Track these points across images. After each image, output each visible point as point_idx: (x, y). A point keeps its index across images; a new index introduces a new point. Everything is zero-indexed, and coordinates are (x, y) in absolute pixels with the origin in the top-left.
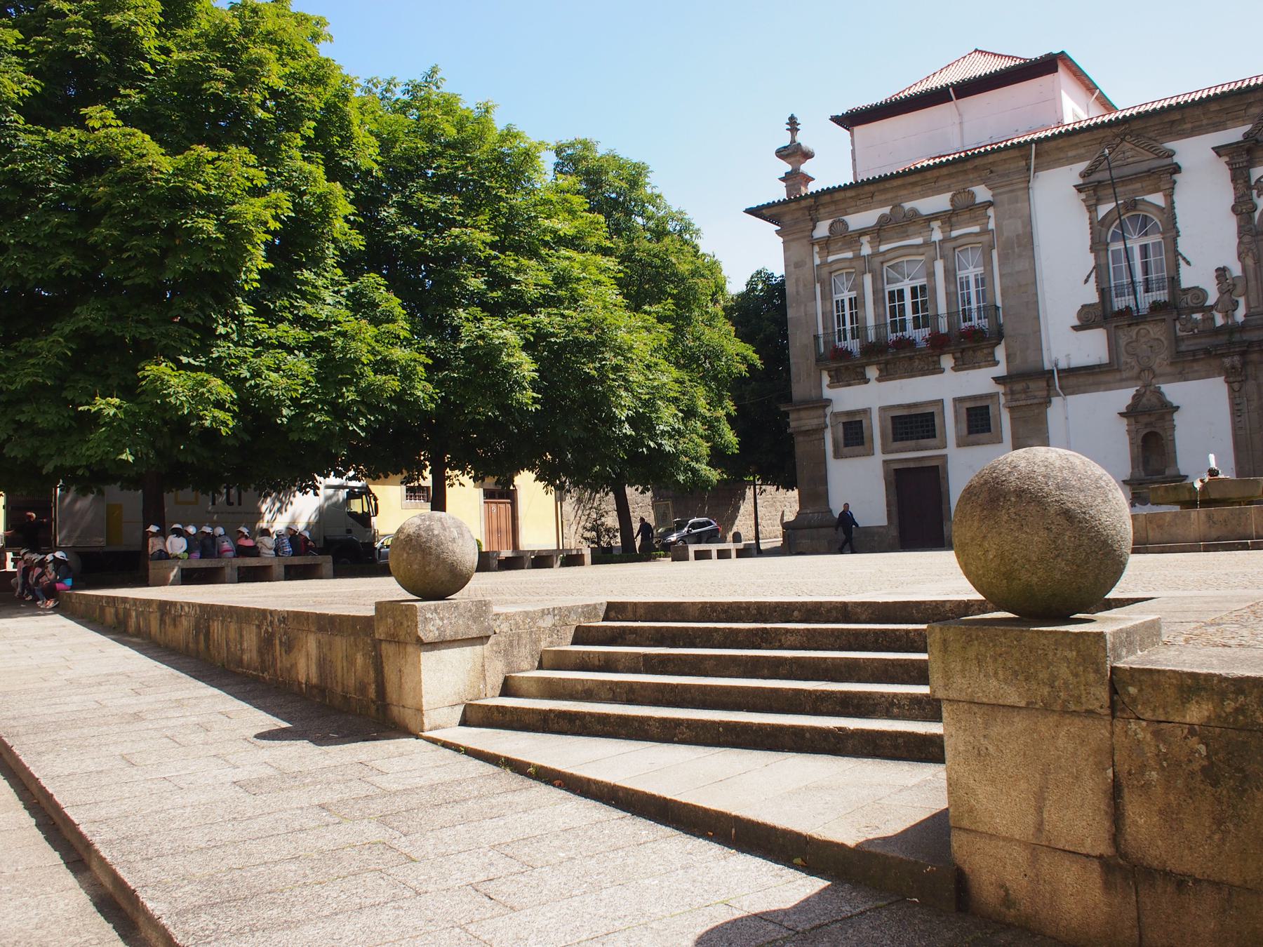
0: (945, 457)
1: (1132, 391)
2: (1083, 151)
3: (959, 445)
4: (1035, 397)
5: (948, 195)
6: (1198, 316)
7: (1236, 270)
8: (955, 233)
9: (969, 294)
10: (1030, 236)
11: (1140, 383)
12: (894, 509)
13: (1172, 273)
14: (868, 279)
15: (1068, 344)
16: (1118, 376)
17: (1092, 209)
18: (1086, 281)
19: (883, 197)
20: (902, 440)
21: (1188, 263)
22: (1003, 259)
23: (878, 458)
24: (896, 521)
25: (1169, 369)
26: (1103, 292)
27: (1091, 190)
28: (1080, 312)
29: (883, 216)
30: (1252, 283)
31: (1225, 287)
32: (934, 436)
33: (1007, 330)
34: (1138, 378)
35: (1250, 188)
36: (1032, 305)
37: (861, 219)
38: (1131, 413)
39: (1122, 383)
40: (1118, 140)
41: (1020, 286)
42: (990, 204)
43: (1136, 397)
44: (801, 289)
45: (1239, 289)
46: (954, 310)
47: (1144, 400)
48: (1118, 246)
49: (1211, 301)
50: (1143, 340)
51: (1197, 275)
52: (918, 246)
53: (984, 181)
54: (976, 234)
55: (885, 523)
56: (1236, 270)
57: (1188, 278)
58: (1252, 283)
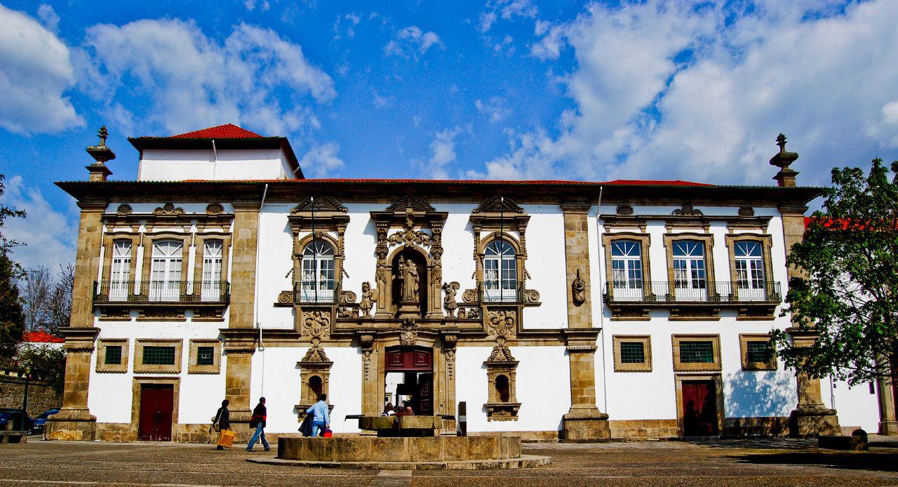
0: (177, 379)
1: (307, 349)
5: (206, 205)
6: (350, 309)
7: (374, 286)
12: (137, 412)
13: (337, 281)
14: (141, 250)
20: (149, 363)
21: (348, 277)
22: (237, 252)
23: (130, 375)
24: (137, 420)
26: (296, 285)
27: (296, 223)
28: (281, 294)
30: (382, 294)
31: (366, 294)
32: (173, 363)
33: (233, 299)
36: (252, 286)
37: (139, 209)
41: (245, 272)
43: (310, 353)
44: (90, 247)
46: (198, 280)
48: (310, 258)
51: (352, 284)
55: (129, 421)
56: (374, 286)
57: (346, 286)
58: (382, 294)
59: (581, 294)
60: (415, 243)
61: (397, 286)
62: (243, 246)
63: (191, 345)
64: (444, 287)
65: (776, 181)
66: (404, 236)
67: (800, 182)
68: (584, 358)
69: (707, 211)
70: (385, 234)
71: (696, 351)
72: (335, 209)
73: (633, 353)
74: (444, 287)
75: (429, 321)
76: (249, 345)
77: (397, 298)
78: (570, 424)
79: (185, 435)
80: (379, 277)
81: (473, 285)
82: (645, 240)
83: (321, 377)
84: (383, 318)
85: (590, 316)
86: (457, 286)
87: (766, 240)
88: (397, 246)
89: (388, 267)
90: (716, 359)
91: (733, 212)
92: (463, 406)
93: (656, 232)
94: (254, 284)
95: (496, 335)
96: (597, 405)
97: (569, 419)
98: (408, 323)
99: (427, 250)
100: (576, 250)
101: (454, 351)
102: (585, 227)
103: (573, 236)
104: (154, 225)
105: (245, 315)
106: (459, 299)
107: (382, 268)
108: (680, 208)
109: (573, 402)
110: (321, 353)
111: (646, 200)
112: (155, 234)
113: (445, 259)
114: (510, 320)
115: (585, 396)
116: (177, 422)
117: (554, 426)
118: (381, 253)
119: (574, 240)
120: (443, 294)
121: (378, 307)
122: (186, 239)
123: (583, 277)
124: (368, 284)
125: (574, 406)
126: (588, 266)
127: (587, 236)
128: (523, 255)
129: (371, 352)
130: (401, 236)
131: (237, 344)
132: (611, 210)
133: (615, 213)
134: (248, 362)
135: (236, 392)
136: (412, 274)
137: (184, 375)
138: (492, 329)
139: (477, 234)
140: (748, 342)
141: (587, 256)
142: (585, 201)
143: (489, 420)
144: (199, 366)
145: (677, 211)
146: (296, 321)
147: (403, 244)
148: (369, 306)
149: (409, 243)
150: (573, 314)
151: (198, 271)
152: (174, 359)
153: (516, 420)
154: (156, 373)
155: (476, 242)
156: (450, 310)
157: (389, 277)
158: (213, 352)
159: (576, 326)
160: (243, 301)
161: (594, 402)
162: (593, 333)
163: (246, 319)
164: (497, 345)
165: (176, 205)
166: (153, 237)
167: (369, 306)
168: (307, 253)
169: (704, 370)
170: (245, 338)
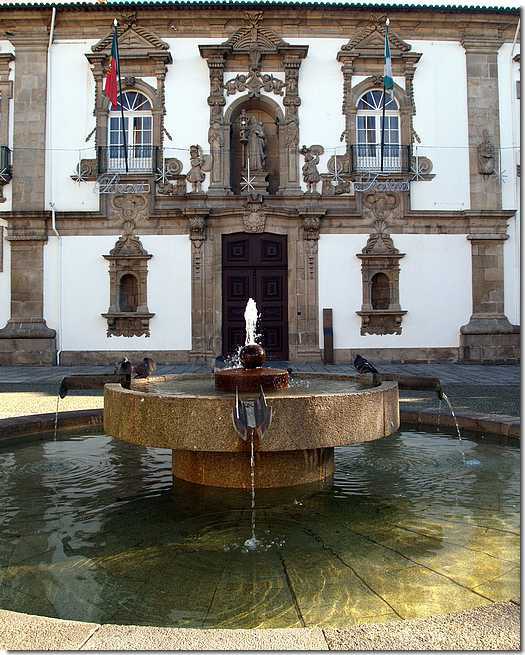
1: (116, 238)
4: (34, 234)
6: (174, 182)
7: (206, 148)
11: (123, 232)
15: (66, 192)
18: (87, 140)
22: (19, 107)
25: (148, 223)
26: (100, 150)
30: (217, 162)
34: (122, 228)
35: (222, 86)
39: (108, 231)
40: (126, 26)
41: (30, 134)
42: (11, 58)
43: (119, 244)
45: (207, 166)
48: (117, 114)
51: (176, 148)
56: (206, 148)
58: (217, 162)
60: (263, 92)
61: (236, 144)
64: (303, 152)
74: (305, 151)
75: (281, 198)
78: (472, 339)
80: (211, 140)
83: (136, 275)
84: (220, 194)
85: (499, 196)
92: (328, 313)
95: (374, 218)
96: (507, 313)
99: (278, 100)
100: (482, 104)
102: (494, 72)
103: (477, 84)
105: (32, 193)
106: (322, 168)
107: (216, 126)
110: (138, 243)
114: (392, 198)
118: (216, 102)
120: (302, 162)
121: (212, 180)
123: (493, 141)
126: (497, 126)
127: (497, 84)
139: (347, 77)
141: (497, 113)
143: (362, 334)
147: (246, 92)
150: (477, 191)
153: (399, 333)
155: (347, 87)
159: (480, 207)
161: (501, 309)
163: (34, 197)
164: (374, 231)
168: (115, 108)
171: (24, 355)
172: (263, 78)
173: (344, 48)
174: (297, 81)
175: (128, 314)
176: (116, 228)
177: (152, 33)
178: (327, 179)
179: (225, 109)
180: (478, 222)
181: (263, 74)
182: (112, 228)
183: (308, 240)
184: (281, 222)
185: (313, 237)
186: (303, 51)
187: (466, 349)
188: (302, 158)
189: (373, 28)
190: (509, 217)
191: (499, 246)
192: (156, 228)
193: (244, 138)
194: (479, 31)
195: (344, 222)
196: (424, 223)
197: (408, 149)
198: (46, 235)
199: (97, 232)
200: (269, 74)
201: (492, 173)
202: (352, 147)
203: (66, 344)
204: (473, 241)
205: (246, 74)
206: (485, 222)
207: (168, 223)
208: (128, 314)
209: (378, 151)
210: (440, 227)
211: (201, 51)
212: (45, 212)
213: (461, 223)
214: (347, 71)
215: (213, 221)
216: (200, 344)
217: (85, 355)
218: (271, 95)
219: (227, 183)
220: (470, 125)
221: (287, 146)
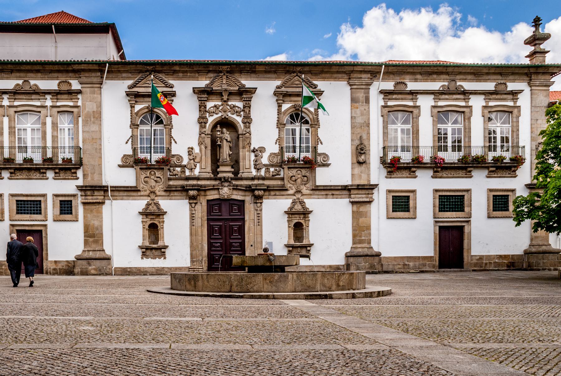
1: (145, 202)
2: (130, 75)
3: (54, 221)
5: (58, 82)
6: (179, 169)
7: (197, 150)
8: (59, 104)
9: (64, 138)
10: (100, 113)
11: (149, 198)
13: (168, 146)
15: (115, 175)
16: (139, 194)
17: (132, 107)
18: (127, 143)
19: (18, 74)
20: (21, 213)
21: (176, 142)
22: (85, 122)
23: (7, 222)
25: (163, 193)
26: (134, 150)
28: (123, 157)
29: (18, 85)
30: (203, 157)
31: (191, 157)
33: (85, 161)
34: (149, 196)
35: (206, 111)
36: (99, 150)
38: (145, 214)
41: (93, 139)
42: (80, 92)
43: (148, 205)
46: (56, 146)
47: (151, 207)
49: (185, 162)
50: (152, 177)
51: (179, 149)
52: (38, 107)
53: (75, 78)
54: (71, 107)
56: (197, 150)
59: (363, 157)
60: (229, 114)
61: (215, 147)
62: (90, 118)
63: (53, 199)
64: (253, 151)
65: (528, 59)
66: (221, 108)
67: (549, 59)
68: (362, 209)
69: (468, 86)
70: (205, 107)
71: (452, 202)
72: (163, 85)
73: (401, 204)
75: (242, 179)
76: (100, 199)
77: (216, 162)
78: (351, 260)
79: (54, 269)
80: (200, 144)
81: (276, 149)
82: (415, 111)
84: (205, 176)
85: (369, 175)
86: (263, 150)
87: (515, 111)
88: (215, 116)
89: (208, 134)
90: (466, 209)
91: (490, 86)
93: (425, 103)
94: (101, 149)
95: (294, 190)
96: (372, 245)
97: (351, 256)
98: (226, 180)
99: (238, 119)
100: (360, 120)
101: (261, 203)
102: (367, 100)
103: (357, 108)
104: (15, 99)
106: (265, 160)
107: (203, 135)
108: (446, 84)
109: (354, 243)
110: (157, 205)
111: (419, 77)
112: (16, 107)
113: (253, 128)
114: (305, 178)
115: (363, 238)
116: (47, 259)
117: (340, 261)
118: (202, 121)
119: (358, 111)
120: (253, 157)
122: (43, 111)
123: (365, 143)
124: (192, 149)
125: (354, 246)
126: (369, 133)
127: (369, 108)
128: (316, 125)
129: (196, 203)
130: (218, 108)
131: (91, 197)
132: (389, 85)
133: (392, 88)
134: (100, 212)
135: (93, 236)
136: (226, 140)
137: (50, 222)
138: (291, 185)
139: (280, 106)
140: (494, 196)
141: (368, 125)
142: (368, 78)
144: (62, 216)
145: (443, 86)
146: (137, 179)
147: (220, 115)
148: (193, 167)
149: (225, 115)
151: (55, 138)
152: (41, 210)
154: (28, 221)
156: (258, 170)
157: (208, 141)
158: (71, 204)
159: (357, 182)
160: (93, 163)
162: (371, 188)
164: (295, 198)
165: (32, 82)
166: (15, 109)
167: (193, 167)
169: (457, 218)
170: (96, 193)
171: (94, 269)
172: (230, 106)
173: (278, 87)
174: (250, 108)
175: (153, 246)
176: (145, 196)
177: (164, 78)
178: (267, 167)
179: (208, 125)
180: (356, 192)
181: (230, 103)
182: (141, 196)
183: (257, 203)
184: (241, 193)
185: (260, 201)
186: (252, 91)
187: (348, 266)
188: (253, 155)
189: (295, 74)
190: (373, 189)
191: (368, 205)
192: (168, 196)
193: (219, 143)
194: (359, 76)
195: (277, 193)
196: (324, 193)
197: (315, 148)
198: (104, 199)
199: (134, 198)
200: (234, 103)
201: (364, 162)
202: (282, 148)
203: (117, 263)
204: (353, 203)
205: (220, 103)
206: (360, 192)
207: (176, 194)
208: (153, 246)
209: (298, 150)
210: (333, 195)
211: (194, 91)
212: (104, 187)
213: (346, 192)
214: (279, 102)
215: (202, 193)
216: (195, 263)
217: (129, 270)
218: (234, 116)
219: (209, 169)
220: (352, 133)
221: (244, 148)
